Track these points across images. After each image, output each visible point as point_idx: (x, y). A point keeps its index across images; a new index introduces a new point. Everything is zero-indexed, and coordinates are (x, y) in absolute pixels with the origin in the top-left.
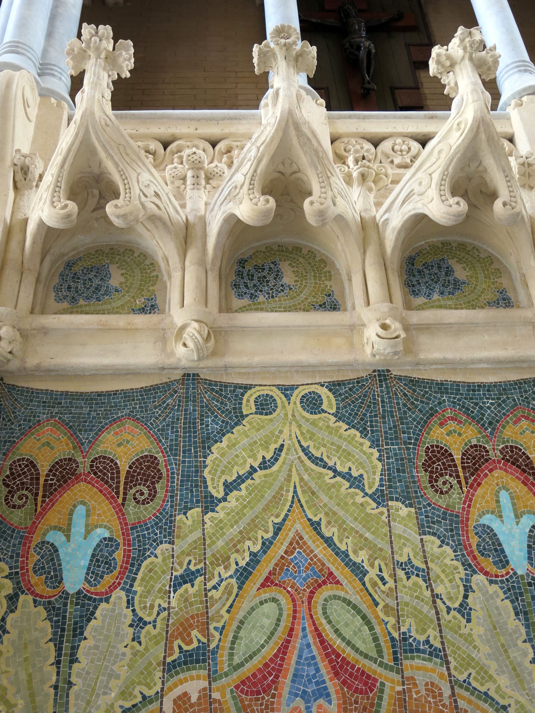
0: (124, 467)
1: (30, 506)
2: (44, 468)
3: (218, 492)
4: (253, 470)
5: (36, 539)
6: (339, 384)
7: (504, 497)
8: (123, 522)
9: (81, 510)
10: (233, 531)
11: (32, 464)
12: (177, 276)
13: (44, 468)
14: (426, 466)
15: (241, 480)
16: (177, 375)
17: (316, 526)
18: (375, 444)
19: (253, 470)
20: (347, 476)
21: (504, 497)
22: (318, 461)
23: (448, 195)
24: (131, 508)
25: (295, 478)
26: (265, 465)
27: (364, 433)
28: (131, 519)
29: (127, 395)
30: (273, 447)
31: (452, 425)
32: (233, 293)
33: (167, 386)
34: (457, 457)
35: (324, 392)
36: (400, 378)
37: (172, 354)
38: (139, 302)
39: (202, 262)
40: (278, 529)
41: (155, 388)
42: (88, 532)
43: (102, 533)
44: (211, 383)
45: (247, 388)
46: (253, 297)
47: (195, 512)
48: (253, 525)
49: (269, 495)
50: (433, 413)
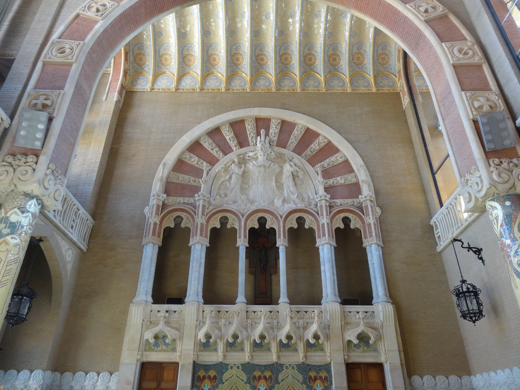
0: (212, 377)
1: (200, 383)
2: (201, 377)
3: (224, 382)
4: (229, 378)
5: (201, 387)
6: (242, 364)
7: (262, 384)
8: (212, 385)
9: (206, 383)
10: (226, 387)
11: (200, 376)
12: (220, 345)
13: (201, 377)
14: (252, 378)
15: (227, 379)
16: (220, 362)
17: (237, 387)
18: (246, 374)
19: (229, 378)
20: (242, 380)
21: (262, 384)
22: (238, 377)
23: (258, 338)
24: (213, 383)
25: (235, 380)
26: (231, 377)
27: (245, 373)
28: (213, 385)
29: (213, 365)
30: (232, 374)
31: (257, 372)
32: (228, 347)
33: (218, 364)
34: (257, 377)
35: (240, 366)
36: (251, 363)
37: (219, 359)
38: (214, 349)
39: (223, 344)
40: (232, 387)
41: (216, 364)
42: (207, 386)
43: (209, 387)
44: (224, 363)
45: (229, 364)
46: (231, 348)
47: (221, 384)
48: (229, 387)
49: (231, 382)
50: (255, 370)
